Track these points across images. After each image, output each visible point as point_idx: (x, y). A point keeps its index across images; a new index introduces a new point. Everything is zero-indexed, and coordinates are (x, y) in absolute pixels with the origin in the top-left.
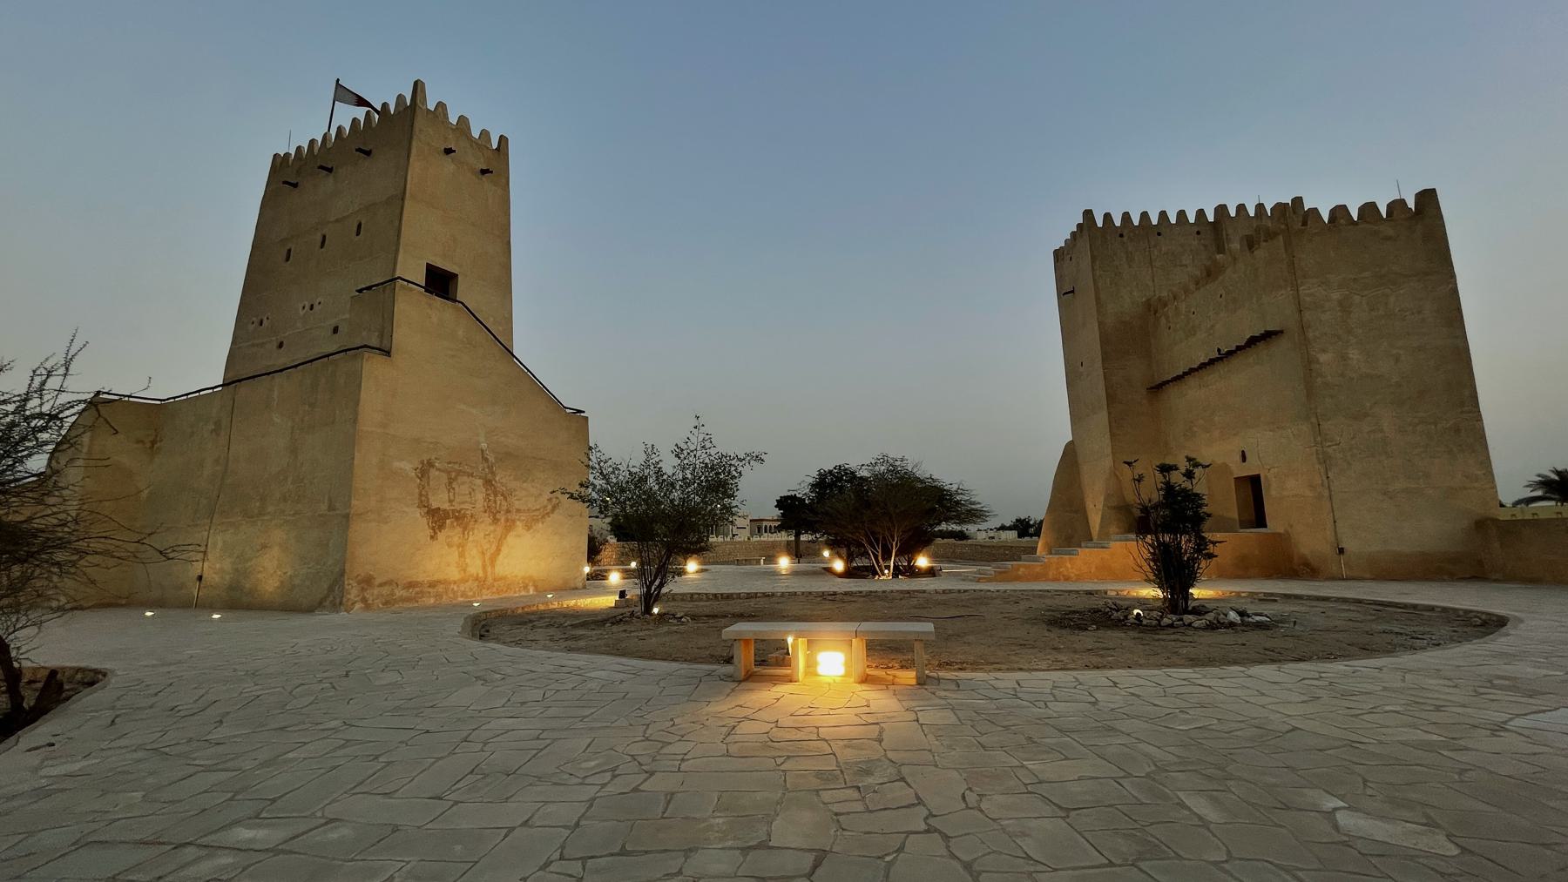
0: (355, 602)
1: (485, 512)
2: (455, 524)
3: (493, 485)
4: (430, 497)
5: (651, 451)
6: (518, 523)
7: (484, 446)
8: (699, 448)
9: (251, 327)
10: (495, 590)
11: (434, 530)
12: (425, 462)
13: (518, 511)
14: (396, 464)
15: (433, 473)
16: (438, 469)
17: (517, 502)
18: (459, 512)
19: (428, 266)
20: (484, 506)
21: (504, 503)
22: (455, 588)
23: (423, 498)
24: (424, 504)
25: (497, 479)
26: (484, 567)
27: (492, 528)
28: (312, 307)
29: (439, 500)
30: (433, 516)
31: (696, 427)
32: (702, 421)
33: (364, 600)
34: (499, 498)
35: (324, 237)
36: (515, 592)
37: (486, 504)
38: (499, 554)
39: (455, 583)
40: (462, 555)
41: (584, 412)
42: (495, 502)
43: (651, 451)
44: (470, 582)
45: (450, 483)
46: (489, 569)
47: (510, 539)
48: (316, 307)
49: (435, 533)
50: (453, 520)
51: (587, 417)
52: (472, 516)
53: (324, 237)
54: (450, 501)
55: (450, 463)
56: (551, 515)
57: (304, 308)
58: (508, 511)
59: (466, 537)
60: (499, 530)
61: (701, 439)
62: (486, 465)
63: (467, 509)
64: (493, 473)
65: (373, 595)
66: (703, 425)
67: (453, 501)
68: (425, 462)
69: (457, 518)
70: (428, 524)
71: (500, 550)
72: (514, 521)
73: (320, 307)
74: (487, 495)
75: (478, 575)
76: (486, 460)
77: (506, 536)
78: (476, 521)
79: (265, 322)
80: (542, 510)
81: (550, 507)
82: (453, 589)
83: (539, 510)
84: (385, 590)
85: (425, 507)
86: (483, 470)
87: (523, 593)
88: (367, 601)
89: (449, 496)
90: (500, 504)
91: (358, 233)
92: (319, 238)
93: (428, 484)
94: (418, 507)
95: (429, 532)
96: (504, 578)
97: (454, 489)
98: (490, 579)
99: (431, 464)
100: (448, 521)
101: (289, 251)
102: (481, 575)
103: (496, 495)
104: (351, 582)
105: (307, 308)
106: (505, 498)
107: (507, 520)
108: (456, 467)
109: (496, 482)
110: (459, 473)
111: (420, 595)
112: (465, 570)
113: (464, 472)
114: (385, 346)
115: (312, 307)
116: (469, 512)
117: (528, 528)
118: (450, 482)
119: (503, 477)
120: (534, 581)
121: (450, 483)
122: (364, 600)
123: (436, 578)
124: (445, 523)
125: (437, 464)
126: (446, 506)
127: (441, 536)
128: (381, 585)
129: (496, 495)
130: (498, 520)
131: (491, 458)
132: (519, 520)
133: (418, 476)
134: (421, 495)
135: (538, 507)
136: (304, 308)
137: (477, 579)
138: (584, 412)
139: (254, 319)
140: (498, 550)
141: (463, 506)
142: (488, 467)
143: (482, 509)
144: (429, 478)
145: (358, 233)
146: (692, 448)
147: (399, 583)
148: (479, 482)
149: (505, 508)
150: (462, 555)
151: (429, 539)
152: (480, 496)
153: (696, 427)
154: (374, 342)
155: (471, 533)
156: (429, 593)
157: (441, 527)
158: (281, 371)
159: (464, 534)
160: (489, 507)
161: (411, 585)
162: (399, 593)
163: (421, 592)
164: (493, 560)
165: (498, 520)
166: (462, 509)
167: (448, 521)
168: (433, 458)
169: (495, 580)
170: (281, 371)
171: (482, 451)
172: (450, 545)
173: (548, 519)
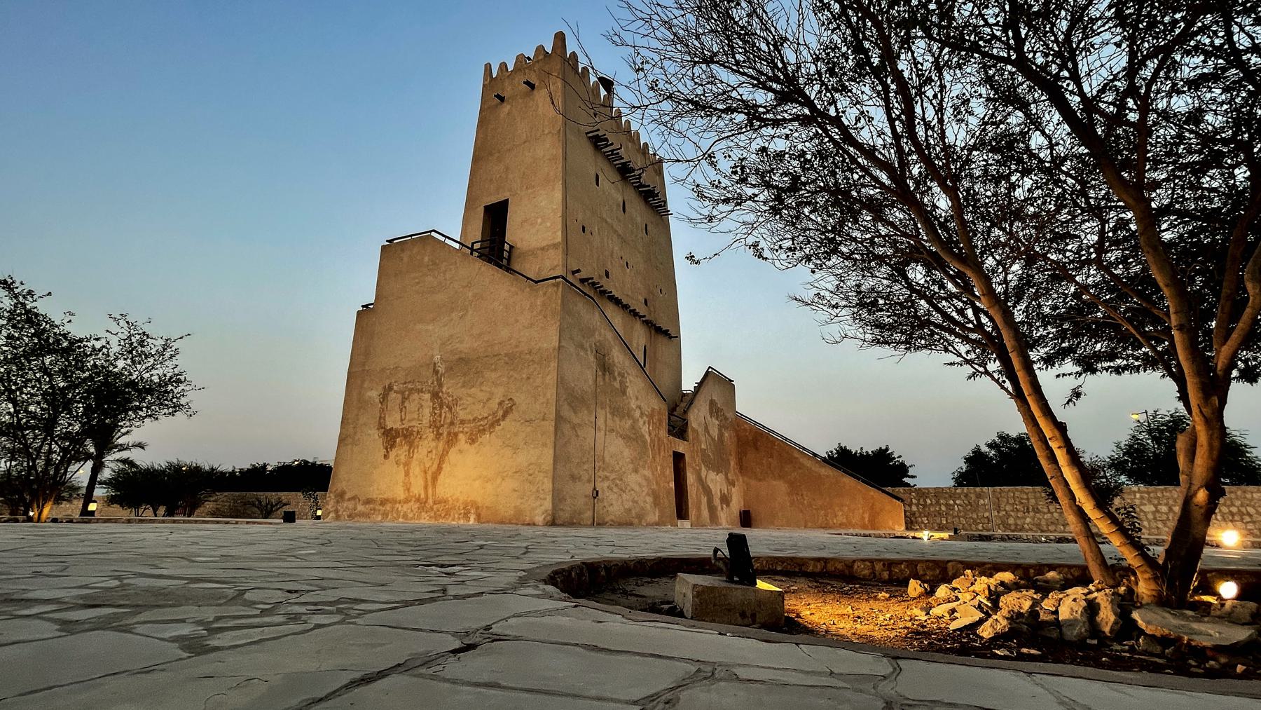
3: (440, 398)
6: (461, 436)
7: (437, 358)
10: (432, 514)
11: (386, 449)
13: (462, 422)
15: (392, 395)
17: (461, 413)
18: (407, 430)
21: (449, 415)
22: (400, 509)
24: (381, 426)
26: (426, 488)
27: (434, 444)
29: (393, 422)
30: (387, 436)
33: (337, 511)
34: (445, 409)
36: (453, 520)
40: (407, 474)
42: (440, 415)
44: (413, 502)
45: (403, 402)
47: (453, 455)
49: (388, 452)
54: (402, 420)
55: (405, 383)
56: (502, 423)
58: (452, 423)
60: (441, 445)
63: (414, 426)
64: (441, 385)
65: (342, 508)
69: (405, 437)
71: (441, 468)
72: (456, 435)
74: (434, 408)
75: (420, 495)
77: (447, 453)
78: (420, 438)
81: (501, 413)
83: (486, 418)
84: (351, 505)
86: (432, 383)
87: (462, 522)
90: (445, 417)
94: (378, 429)
96: (446, 501)
97: (405, 407)
98: (430, 501)
99: (390, 388)
100: (398, 440)
102: (423, 496)
106: (450, 409)
107: (449, 434)
108: (410, 386)
109: (442, 392)
116: (415, 429)
117: (472, 441)
118: (404, 399)
119: (450, 387)
120: (477, 508)
121: (403, 402)
122: (337, 511)
123: (385, 496)
124: (395, 442)
126: (398, 426)
127: (392, 454)
129: (441, 408)
130: (441, 434)
131: (441, 369)
132: (462, 432)
134: (380, 418)
135: (486, 415)
137: (418, 500)
140: (440, 468)
143: (428, 425)
148: (427, 396)
149: (448, 421)
150: (407, 474)
155: (416, 451)
157: (392, 446)
162: (360, 508)
163: (374, 509)
164: (435, 478)
166: (410, 427)
169: (435, 503)
171: (435, 364)
172: (397, 463)
173: (498, 428)
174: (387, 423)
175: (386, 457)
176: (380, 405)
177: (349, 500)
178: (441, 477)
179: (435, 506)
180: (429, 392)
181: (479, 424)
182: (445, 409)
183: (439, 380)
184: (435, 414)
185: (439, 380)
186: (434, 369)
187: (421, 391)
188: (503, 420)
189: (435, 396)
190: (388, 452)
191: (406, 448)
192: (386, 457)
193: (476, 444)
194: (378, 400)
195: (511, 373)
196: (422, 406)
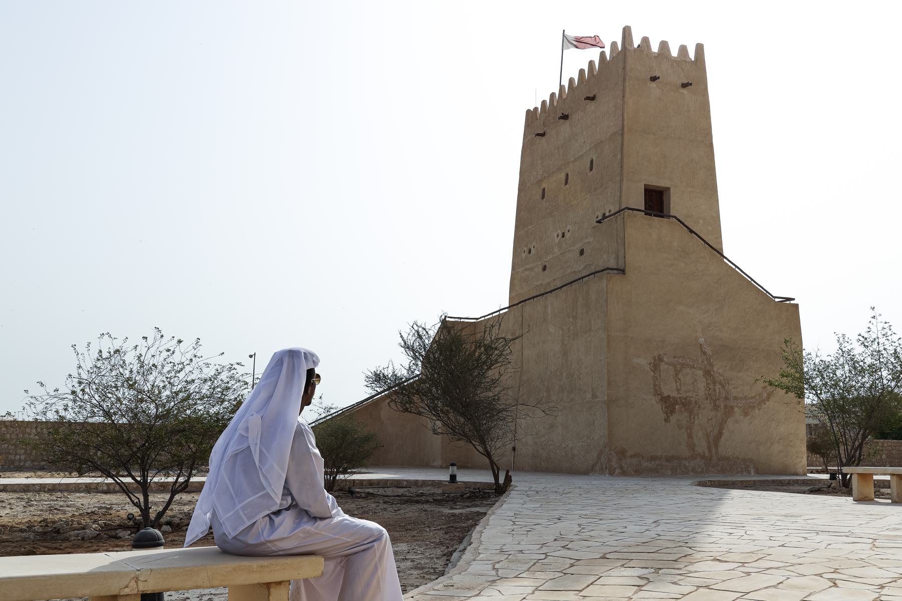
0: (615, 469)
1: (707, 399)
2: (683, 410)
3: (713, 376)
4: (662, 386)
5: (842, 339)
6: (736, 409)
7: (702, 340)
8: (880, 336)
9: (524, 255)
10: (719, 468)
11: (667, 414)
12: (656, 357)
13: (735, 398)
14: (636, 361)
15: (663, 366)
16: (666, 363)
18: (685, 399)
19: (645, 185)
20: (705, 394)
21: (723, 391)
22: (687, 464)
23: (657, 388)
24: (657, 392)
25: (715, 369)
26: (709, 448)
28: (563, 236)
29: (669, 389)
31: (874, 317)
32: (877, 312)
33: (621, 467)
34: (718, 386)
35: (567, 175)
37: (707, 392)
38: (721, 437)
39: (686, 459)
41: (793, 299)
42: (715, 390)
43: (842, 339)
45: (677, 375)
46: (714, 450)
48: (567, 235)
49: (668, 416)
50: (680, 406)
51: (798, 305)
52: (696, 402)
53: (567, 175)
54: (678, 390)
55: (675, 357)
56: (767, 403)
57: (558, 236)
58: (726, 398)
59: (692, 420)
61: (880, 328)
62: (705, 357)
64: (711, 365)
66: (880, 315)
67: (680, 390)
68: (656, 357)
69: (684, 405)
70: (662, 409)
72: (732, 408)
73: (569, 234)
74: (708, 384)
76: (705, 353)
77: (726, 422)
79: (533, 252)
80: (757, 397)
81: (765, 395)
82: (685, 465)
85: (658, 395)
86: (702, 362)
88: (623, 468)
89: (677, 386)
90: (719, 392)
91: (591, 169)
92: (562, 176)
93: (660, 376)
95: (663, 416)
99: (660, 359)
101: (544, 189)
102: (707, 454)
103: (714, 383)
104: (612, 452)
105: (560, 236)
106: (723, 387)
107: (726, 407)
108: (680, 360)
109: (713, 371)
110: (683, 365)
111: (660, 467)
112: (693, 450)
113: (688, 365)
114: (621, 267)
115: (563, 236)
117: (746, 414)
119: (718, 368)
121: (677, 375)
122: (621, 467)
124: (675, 408)
125: (665, 359)
126: (674, 394)
127: (673, 419)
128: (631, 457)
129: (714, 383)
130: (719, 406)
131: (708, 350)
132: (737, 406)
133: (652, 370)
134: (655, 385)
136: (558, 236)
137: (703, 457)
138: (793, 299)
139: (525, 249)
140: (720, 434)
141: (688, 394)
142: (707, 359)
144: (660, 370)
145: (591, 169)
146: (874, 336)
147: (644, 456)
148: (700, 373)
150: (690, 436)
151: (663, 420)
152: (701, 385)
153: (874, 317)
154: (612, 264)
155: (696, 417)
156: (667, 466)
157: (672, 412)
158: (551, 291)
159: (690, 418)
160: (709, 395)
161: (653, 459)
162: (645, 464)
165: (719, 406)
166: (687, 397)
167: (676, 407)
168: (662, 353)
170: (551, 291)
171: (701, 345)
174: (663, 390)
175: (667, 420)
176: (652, 373)
177: (631, 457)
178: (723, 439)
179: (720, 463)
180: (701, 369)
181: (749, 401)
182: (718, 386)
183: (708, 360)
184: (710, 389)
185: (708, 360)
186: (702, 351)
187: (692, 367)
188: (768, 401)
189: (708, 373)
190: (668, 416)
191: (686, 414)
192: (667, 420)
193: (749, 417)
194: (648, 368)
195: (770, 366)
196: (696, 380)
